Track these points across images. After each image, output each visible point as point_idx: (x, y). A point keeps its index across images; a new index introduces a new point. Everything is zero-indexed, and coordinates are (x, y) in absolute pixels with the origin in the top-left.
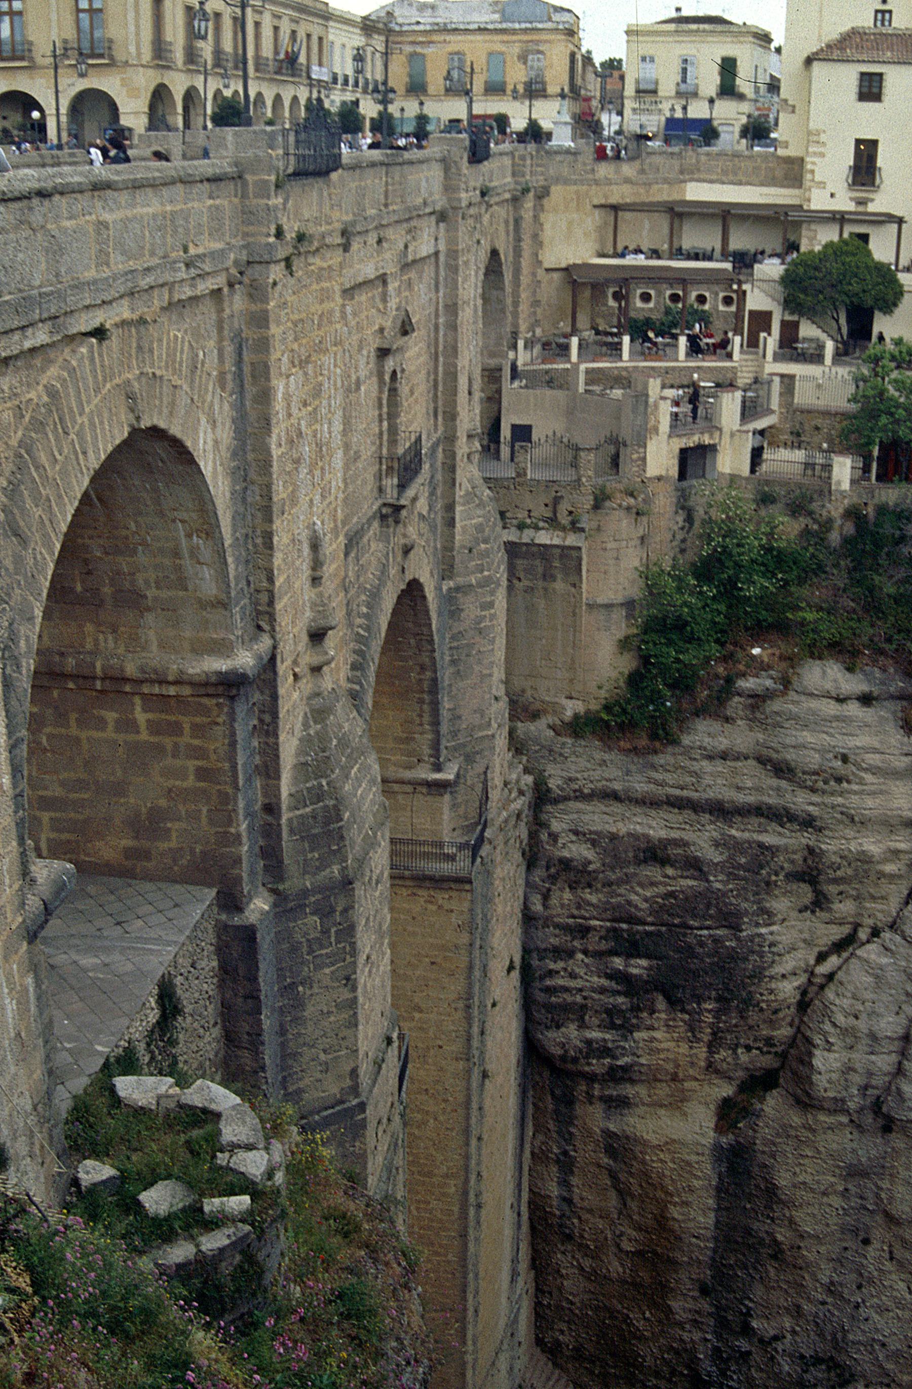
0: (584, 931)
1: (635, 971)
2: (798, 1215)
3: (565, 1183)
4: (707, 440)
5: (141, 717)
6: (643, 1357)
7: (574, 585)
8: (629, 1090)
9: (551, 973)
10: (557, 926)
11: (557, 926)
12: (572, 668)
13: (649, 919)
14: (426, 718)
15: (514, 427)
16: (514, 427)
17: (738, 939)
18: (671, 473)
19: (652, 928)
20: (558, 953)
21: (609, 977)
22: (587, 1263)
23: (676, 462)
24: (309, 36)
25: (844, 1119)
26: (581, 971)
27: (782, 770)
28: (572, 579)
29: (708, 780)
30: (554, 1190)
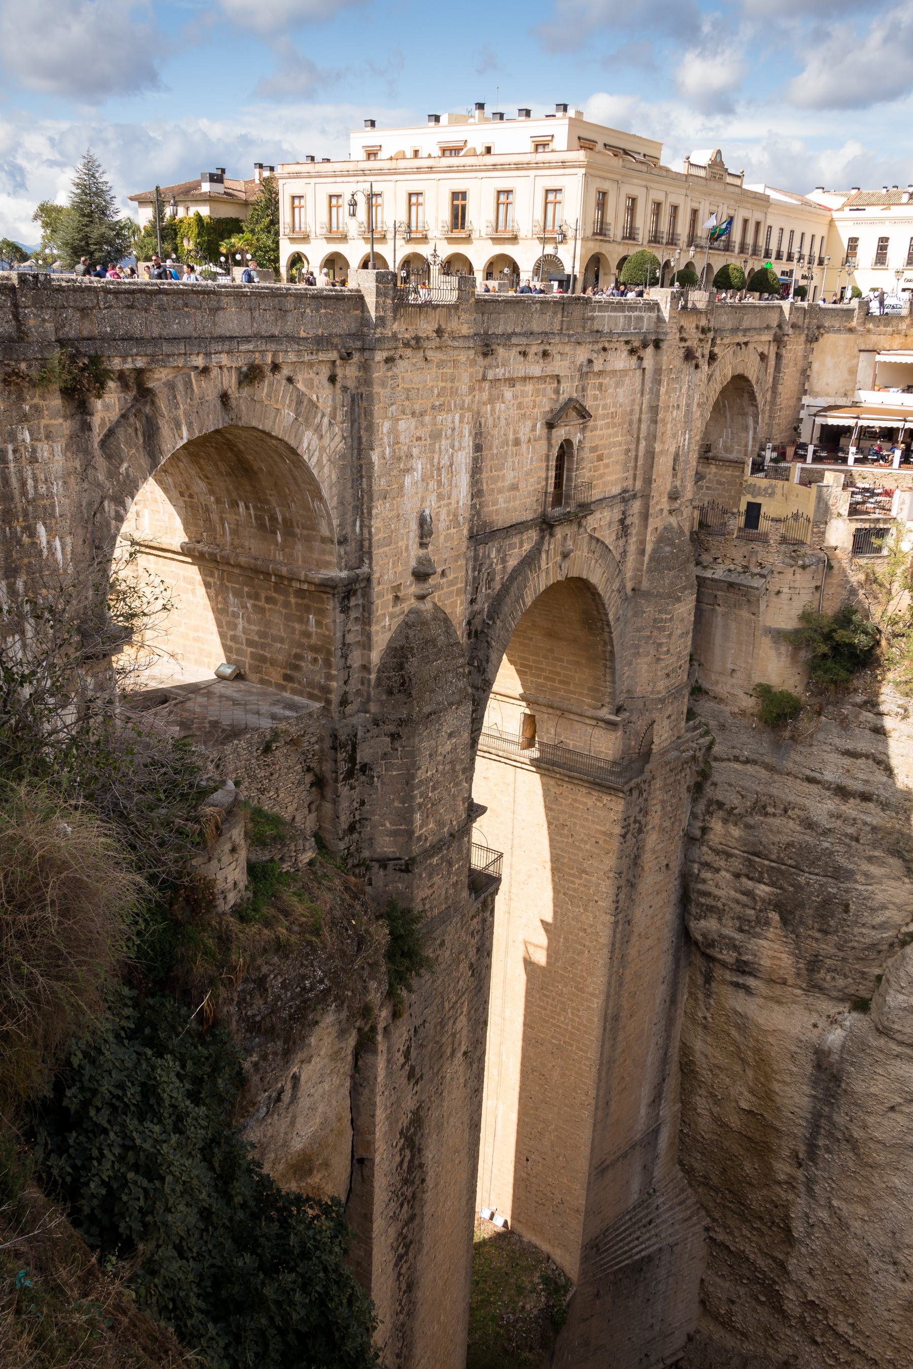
0: (729, 855)
2: (870, 1120)
5: (293, 600)
6: (751, 1201)
7: (754, 614)
8: (751, 982)
9: (704, 881)
15: (749, 504)
16: (749, 504)
18: (845, 545)
19: (773, 864)
21: (744, 893)
22: (716, 1110)
24: (746, 221)
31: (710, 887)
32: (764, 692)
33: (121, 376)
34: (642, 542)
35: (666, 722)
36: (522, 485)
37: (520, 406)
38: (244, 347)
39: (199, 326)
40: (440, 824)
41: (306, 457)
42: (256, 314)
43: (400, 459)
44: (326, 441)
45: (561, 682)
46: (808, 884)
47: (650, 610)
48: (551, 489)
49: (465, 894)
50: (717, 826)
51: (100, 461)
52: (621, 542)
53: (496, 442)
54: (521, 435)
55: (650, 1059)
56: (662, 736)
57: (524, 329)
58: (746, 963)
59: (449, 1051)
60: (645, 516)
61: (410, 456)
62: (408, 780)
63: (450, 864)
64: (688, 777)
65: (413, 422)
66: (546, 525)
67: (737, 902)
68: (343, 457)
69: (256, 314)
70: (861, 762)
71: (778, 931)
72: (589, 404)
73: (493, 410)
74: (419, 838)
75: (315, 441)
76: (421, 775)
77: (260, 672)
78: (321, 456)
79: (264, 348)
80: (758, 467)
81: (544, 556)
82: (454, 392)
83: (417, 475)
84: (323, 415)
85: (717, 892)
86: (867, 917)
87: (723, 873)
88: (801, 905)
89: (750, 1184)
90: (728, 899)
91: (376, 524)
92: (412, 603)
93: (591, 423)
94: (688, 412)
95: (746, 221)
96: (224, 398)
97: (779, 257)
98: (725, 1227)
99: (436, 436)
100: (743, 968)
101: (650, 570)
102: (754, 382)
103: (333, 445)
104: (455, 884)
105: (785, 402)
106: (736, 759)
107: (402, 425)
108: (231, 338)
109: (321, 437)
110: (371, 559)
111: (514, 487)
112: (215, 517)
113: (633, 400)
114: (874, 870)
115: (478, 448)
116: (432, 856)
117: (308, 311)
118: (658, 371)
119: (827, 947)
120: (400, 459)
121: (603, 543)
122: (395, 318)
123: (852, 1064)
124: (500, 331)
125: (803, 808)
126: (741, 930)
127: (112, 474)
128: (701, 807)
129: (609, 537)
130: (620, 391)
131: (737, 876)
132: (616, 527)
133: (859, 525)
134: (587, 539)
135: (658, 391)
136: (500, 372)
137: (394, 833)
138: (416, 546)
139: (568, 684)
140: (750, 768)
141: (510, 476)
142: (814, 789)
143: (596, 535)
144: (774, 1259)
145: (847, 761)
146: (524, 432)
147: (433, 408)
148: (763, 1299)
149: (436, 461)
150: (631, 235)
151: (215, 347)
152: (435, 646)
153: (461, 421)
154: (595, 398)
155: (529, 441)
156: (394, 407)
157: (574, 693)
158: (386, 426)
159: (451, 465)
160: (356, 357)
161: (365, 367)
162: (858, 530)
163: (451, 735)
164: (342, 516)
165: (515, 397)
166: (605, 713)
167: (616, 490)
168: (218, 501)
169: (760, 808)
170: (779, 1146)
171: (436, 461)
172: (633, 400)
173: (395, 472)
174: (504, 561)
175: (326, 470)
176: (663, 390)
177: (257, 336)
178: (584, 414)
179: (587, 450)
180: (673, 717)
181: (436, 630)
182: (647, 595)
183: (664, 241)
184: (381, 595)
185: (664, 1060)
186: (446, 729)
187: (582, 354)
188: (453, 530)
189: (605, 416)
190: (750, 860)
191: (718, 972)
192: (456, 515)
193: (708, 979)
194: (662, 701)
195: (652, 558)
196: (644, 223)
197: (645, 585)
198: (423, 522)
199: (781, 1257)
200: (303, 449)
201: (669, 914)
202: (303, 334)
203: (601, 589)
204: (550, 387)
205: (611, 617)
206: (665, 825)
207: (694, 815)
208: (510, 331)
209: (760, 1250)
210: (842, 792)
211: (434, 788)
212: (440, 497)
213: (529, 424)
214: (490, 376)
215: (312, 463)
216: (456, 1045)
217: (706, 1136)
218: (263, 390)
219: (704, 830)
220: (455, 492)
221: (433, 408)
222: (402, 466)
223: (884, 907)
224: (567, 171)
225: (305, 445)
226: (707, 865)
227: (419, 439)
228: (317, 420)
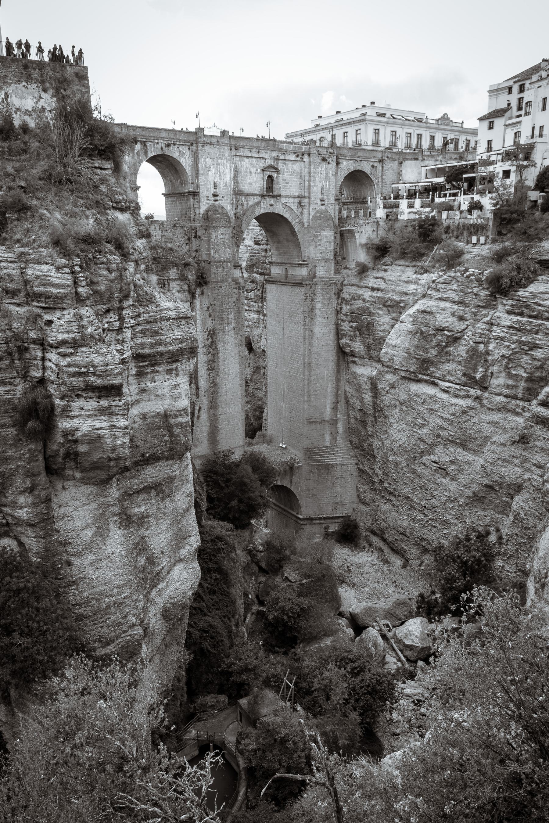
31: (343, 328)
32: (359, 264)
33: (141, 142)
47: (312, 232)
48: (265, 186)
50: (344, 307)
51: (136, 155)
56: (321, 272)
60: (309, 203)
61: (210, 167)
64: (333, 289)
70: (379, 280)
76: (212, 240)
82: (224, 155)
83: (213, 172)
86: (379, 328)
88: (362, 327)
91: (200, 180)
92: (212, 202)
96: (162, 148)
99: (218, 164)
101: (312, 220)
106: (349, 285)
107: (207, 160)
111: (251, 184)
113: (301, 170)
114: (381, 312)
115: (236, 171)
118: (310, 162)
119: (370, 341)
125: (363, 295)
126: (351, 340)
127: (138, 158)
129: (294, 207)
130: (295, 167)
131: (349, 322)
136: (242, 154)
137: (207, 254)
140: (353, 287)
141: (249, 181)
142: (367, 289)
145: (376, 280)
146: (253, 170)
158: (203, 160)
160: (195, 145)
161: (197, 147)
164: (192, 178)
167: (297, 194)
169: (354, 298)
172: (301, 170)
176: (312, 167)
178: (277, 170)
182: (311, 227)
187: (275, 154)
198: (214, 183)
201: (332, 337)
203: (290, 220)
204: (263, 161)
205: (296, 230)
207: (338, 303)
210: (373, 289)
212: (220, 179)
213: (255, 169)
214: (238, 154)
215: (184, 165)
218: (171, 148)
219: (341, 308)
220: (225, 180)
223: (383, 324)
226: (342, 320)
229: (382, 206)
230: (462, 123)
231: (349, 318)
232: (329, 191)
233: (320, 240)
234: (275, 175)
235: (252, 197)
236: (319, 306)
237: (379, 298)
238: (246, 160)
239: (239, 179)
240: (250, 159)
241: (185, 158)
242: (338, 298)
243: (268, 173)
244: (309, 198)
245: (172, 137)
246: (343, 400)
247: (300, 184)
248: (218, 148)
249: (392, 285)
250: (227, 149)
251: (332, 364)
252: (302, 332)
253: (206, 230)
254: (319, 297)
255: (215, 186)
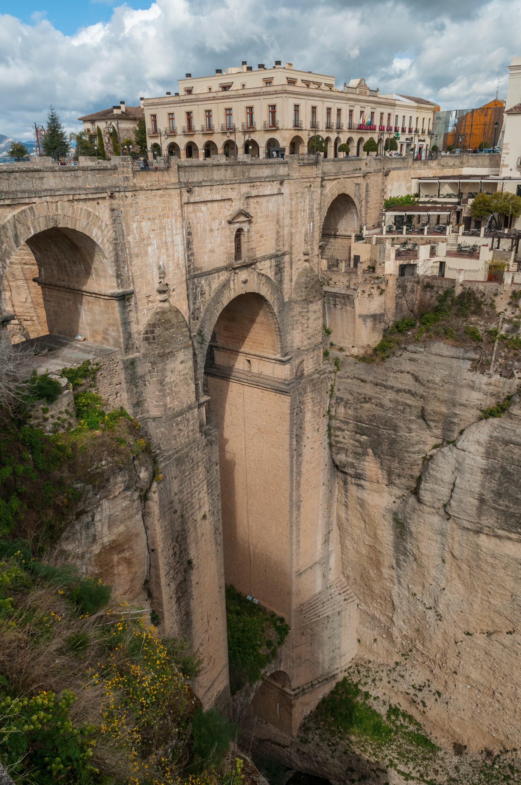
1: (362, 440)
3: (346, 513)
4: (412, 262)
10: (340, 420)
11: (340, 420)
12: (354, 335)
13: (367, 423)
14: (279, 340)
17: (396, 435)
20: (340, 429)
22: (355, 546)
23: (398, 269)
24: (382, 114)
25: (433, 510)
26: (346, 437)
27: (416, 379)
28: (352, 306)
29: (391, 379)
30: (343, 516)
31: (341, 439)
34: (291, 275)
35: (310, 360)
36: (217, 250)
37: (211, 213)
38: (58, 193)
39: (35, 185)
40: (181, 402)
41: (95, 240)
42: (63, 179)
43: (144, 239)
44: (105, 232)
45: (260, 343)
46: (383, 434)
48: (233, 251)
49: (198, 435)
52: (278, 276)
53: (199, 230)
54: (213, 227)
55: (320, 522)
56: (309, 367)
57: (209, 178)
58: (359, 474)
59: (197, 507)
60: (291, 263)
62: (161, 383)
63: (188, 420)
65: (149, 223)
66: (232, 269)
67: (353, 445)
68: (116, 239)
69: (63, 179)
71: (372, 458)
72: (251, 211)
73: (196, 216)
74: (170, 408)
75: (99, 233)
76: (167, 380)
77: (93, 337)
78: (103, 240)
79: (68, 193)
80: (359, 238)
81: (232, 282)
82: (171, 209)
83: (155, 247)
84: (102, 221)
85: (344, 441)
87: (346, 432)
89: (373, 580)
90: (349, 443)
93: (253, 220)
94: (312, 213)
95: (382, 114)
97: (403, 130)
98: (366, 603)
99: (163, 228)
100: (358, 476)
102: (352, 197)
103: (109, 234)
104: (193, 430)
105: (373, 206)
107: (143, 224)
108: (51, 190)
109: (102, 231)
110: (134, 284)
111: (212, 251)
112: (68, 269)
115: (189, 234)
116: (178, 416)
117: (90, 176)
120: (144, 239)
121: (266, 276)
122: (134, 177)
123: (410, 519)
124: (195, 180)
128: (333, 401)
129: (271, 274)
130: (270, 205)
132: (273, 268)
133: (401, 262)
134: (256, 274)
135: (291, 203)
136: (197, 199)
138: (157, 278)
139: (262, 344)
141: (209, 247)
143: (262, 272)
144: (388, 616)
146: (215, 225)
147: (160, 216)
148: (384, 636)
149: (164, 240)
150: (314, 126)
151: (43, 194)
152: (171, 322)
153: (176, 222)
154: (255, 208)
155: (219, 229)
156: (138, 217)
157: (266, 348)
158: (135, 225)
159: (173, 242)
162: (401, 265)
163: (182, 362)
165: (208, 209)
166: (278, 357)
167: (272, 252)
168: (69, 262)
170: (383, 560)
171: (164, 240)
173: (142, 245)
174: (210, 285)
175: (107, 245)
177: (65, 188)
179: (253, 233)
180: (315, 358)
181: (170, 316)
183: (335, 127)
184: (140, 300)
185: (329, 524)
186: (179, 360)
187: (245, 189)
188: (177, 271)
189: (261, 217)
190: (357, 425)
191: (349, 478)
192: (178, 265)
193: (345, 483)
194: (307, 350)
195: (297, 283)
196: (321, 120)
197: (294, 296)
198: (159, 268)
199: (391, 615)
200: (93, 237)
202: (88, 186)
203: (268, 297)
204: (227, 204)
206: (315, 409)
208: (201, 180)
209: (381, 612)
211: (175, 386)
212: (168, 256)
213: (217, 222)
214: (192, 200)
215: (99, 242)
216: (201, 504)
217: (353, 559)
220: (176, 254)
221: (160, 216)
222: (145, 242)
224: (278, 96)
225: (94, 234)
227: (153, 230)
228: (100, 223)
229: (393, 255)
230: (378, 90)
231: (351, 426)
232: (313, 236)
233: (308, 319)
234: (245, 227)
235: (216, 275)
236: (308, 416)
237: (410, 406)
238: (203, 207)
239: (195, 246)
240: (209, 204)
241: (100, 227)
242: (331, 397)
243: (237, 226)
244: (291, 254)
245: (69, 185)
246: (335, 527)
247: (278, 232)
248: (161, 196)
249: (436, 389)
250: (175, 193)
251: (324, 487)
252: (288, 459)
253: (153, 363)
254: (309, 406)
255: (163, 274)
